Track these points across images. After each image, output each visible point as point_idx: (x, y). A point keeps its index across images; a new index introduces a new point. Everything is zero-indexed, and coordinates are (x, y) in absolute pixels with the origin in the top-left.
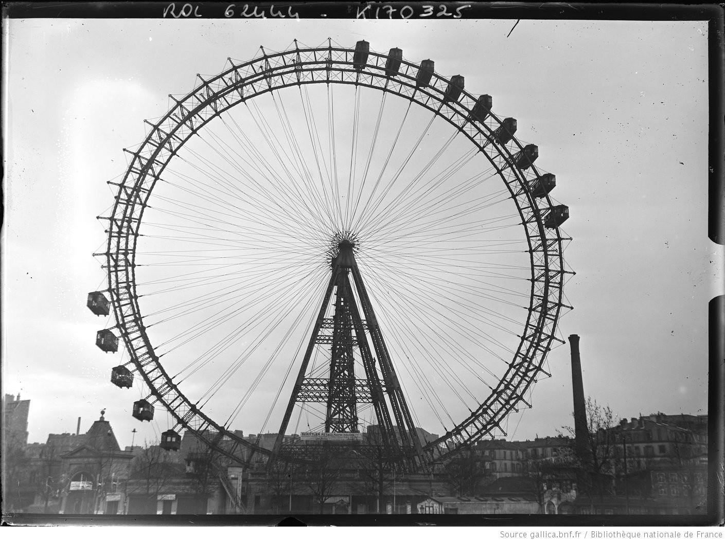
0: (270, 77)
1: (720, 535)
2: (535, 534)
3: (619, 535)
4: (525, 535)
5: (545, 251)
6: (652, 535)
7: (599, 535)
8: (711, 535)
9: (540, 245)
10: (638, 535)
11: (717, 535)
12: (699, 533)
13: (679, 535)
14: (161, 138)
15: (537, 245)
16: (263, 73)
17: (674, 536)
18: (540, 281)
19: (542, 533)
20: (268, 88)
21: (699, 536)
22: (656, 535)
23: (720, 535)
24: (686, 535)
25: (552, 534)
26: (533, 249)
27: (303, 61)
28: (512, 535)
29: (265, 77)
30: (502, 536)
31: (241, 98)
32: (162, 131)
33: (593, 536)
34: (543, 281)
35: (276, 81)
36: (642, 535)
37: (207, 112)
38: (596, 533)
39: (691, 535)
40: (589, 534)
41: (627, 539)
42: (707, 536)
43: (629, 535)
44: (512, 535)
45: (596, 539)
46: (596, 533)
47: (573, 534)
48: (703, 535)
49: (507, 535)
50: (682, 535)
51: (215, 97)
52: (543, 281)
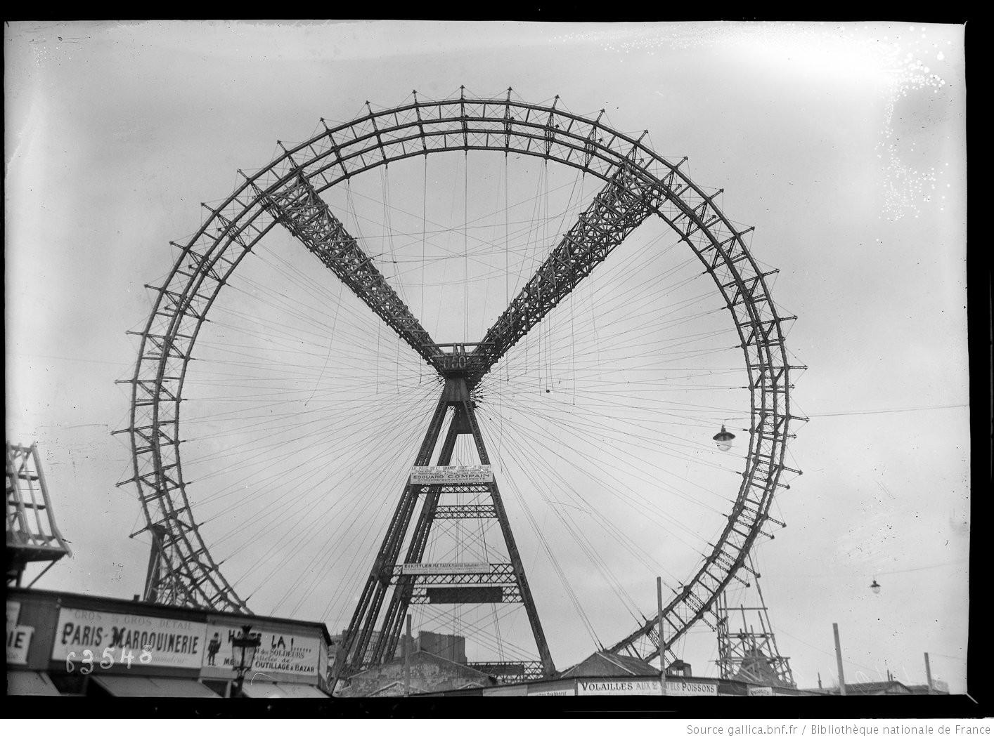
0: (210, 268)
1: (988, 730)
3: (849, 730)
5: (701, 226)
6: (895, 730)
7: (822, 730)
8: (975, 730)
9: (690, 224)
10: (876, 730)
11: (983, 730)
12: (958, 727)
14: (147, 438)
15: (687, 226)
16: (198, 271)
17: (924, 731)
18: (719, 265)
20: (218, 283)
21: (959, 731)
22: (900, 730)
26: (685, 233)
27: (231, 219)
29: (205, 274)
31: (198, 320)
32: (143, 428)
34: (722, 264)
35: (221, 268)
36: (881, 730)
37: (174, 365)
38: (817, 727)
39: (948, 730)
40: (808, 730)
41: (859, 735)
42: (970, 731)
46: (817, 727)
48: (965, 730)
51: (169, 342)
52: (722, 264)
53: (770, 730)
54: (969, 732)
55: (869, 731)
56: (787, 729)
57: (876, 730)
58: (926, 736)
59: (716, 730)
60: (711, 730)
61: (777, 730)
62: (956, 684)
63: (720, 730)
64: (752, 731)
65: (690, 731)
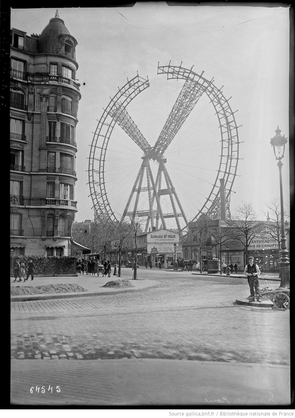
1: (292, 414)
3: (236, 414)
6: (254, 414)
7: (224, 414)
8: (287, 414)
10: (246, 414)
11: (290, 414)
13: (269, 414)
21: (281, 414)
22: (256, 414)
23: (292, 414)
24: (273, 414)
36: (249, 414)
39: (276, 414)
40: (219, 414)
42: (285, 414)
46: (223, 413)
48: (283, 414)
50: (271, 414)
53: (203, 414)
54: (285, 415)
55: (244, 414)
56: (210, 414)
57: (246, 414)
58: (267, 417)
59: (181, 414)
60: (179, 414)
61: (206, 414)
62: (287, 400)
63: (183, 414)
64: (196, 414)
65: (171, 415)
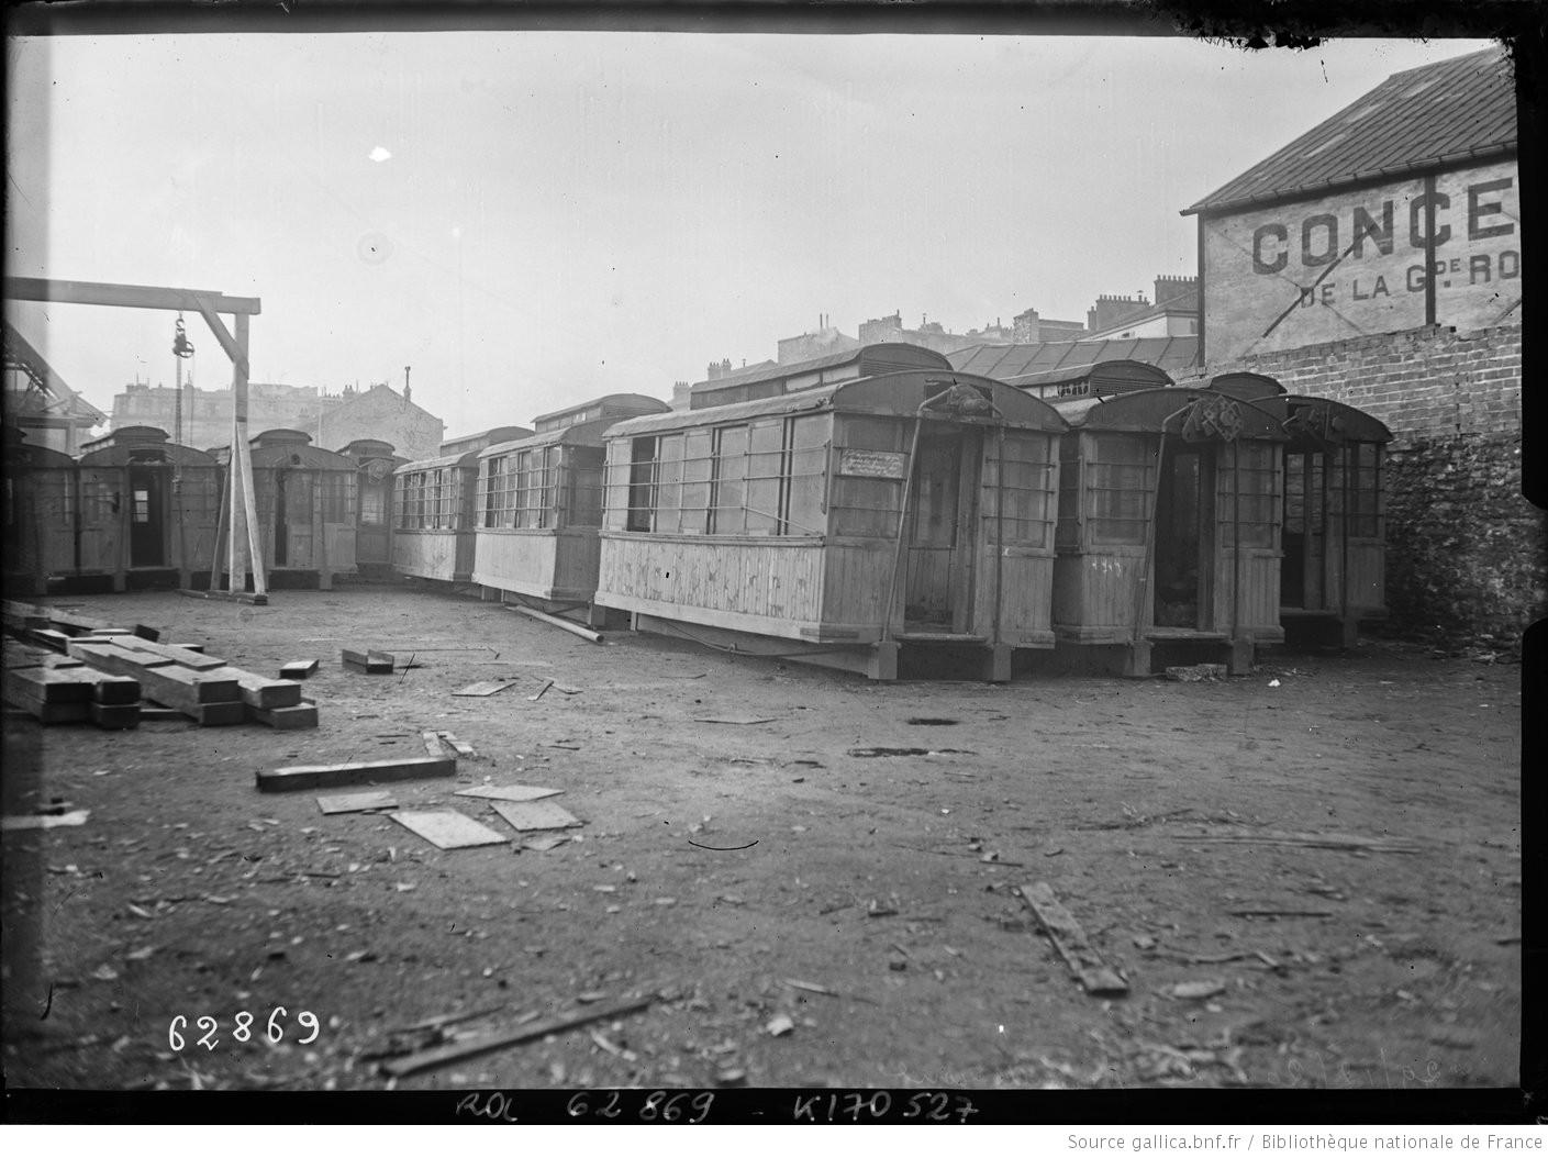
1: (1538, 1143)
2: (1143, 1142)
3: (1321, 1142)
4: (1120, 1142)
6: (1393, 1143)
7: (1279, 1143)
8: (1519, 1142)
10: (1363, 1143)
11: (1531, 1143)
13: (1449, 1143)
17: (1439, 1144)
19: (1158, 1138)
21: (1493, 1144)
22: (1401, 1143)
23: (1538, 1143)
24: (1465, 1143)
25: (1178, 1142)
28: (1094, 1144)
30: (1073, 1144)
33: (1267, 1144)
36: (1371, 1143)
39: (1476, 1143)
40: (1258, 1141)
41: (1338, 1151)
42: (1510, 1144)
43: (1342, 1143)
44: (1094, 1144)
45: (1273, 1152)
47: (1224, 1141)
48: (1502, 1143)
49: (1083, 1143)
50: (1457, 1143)
